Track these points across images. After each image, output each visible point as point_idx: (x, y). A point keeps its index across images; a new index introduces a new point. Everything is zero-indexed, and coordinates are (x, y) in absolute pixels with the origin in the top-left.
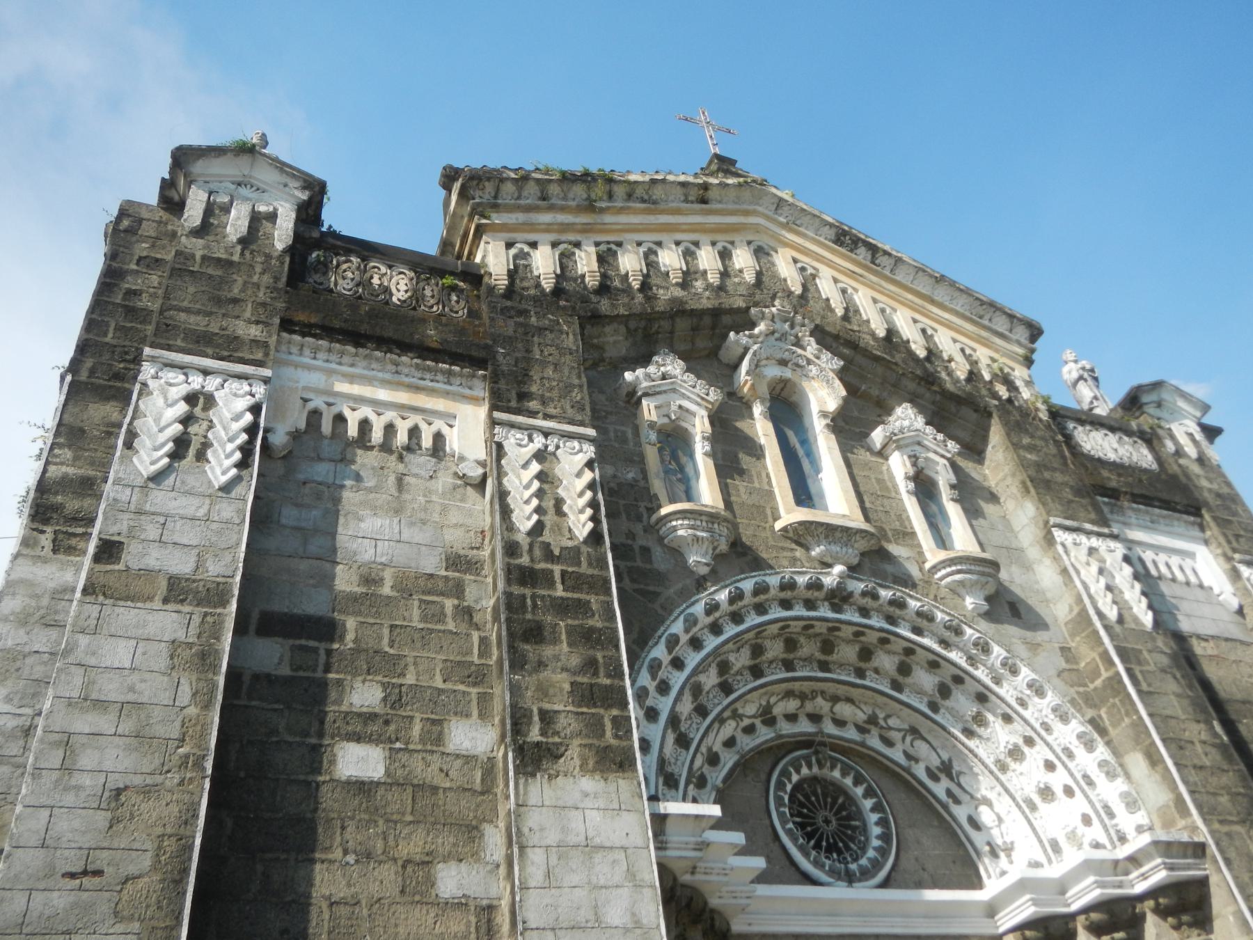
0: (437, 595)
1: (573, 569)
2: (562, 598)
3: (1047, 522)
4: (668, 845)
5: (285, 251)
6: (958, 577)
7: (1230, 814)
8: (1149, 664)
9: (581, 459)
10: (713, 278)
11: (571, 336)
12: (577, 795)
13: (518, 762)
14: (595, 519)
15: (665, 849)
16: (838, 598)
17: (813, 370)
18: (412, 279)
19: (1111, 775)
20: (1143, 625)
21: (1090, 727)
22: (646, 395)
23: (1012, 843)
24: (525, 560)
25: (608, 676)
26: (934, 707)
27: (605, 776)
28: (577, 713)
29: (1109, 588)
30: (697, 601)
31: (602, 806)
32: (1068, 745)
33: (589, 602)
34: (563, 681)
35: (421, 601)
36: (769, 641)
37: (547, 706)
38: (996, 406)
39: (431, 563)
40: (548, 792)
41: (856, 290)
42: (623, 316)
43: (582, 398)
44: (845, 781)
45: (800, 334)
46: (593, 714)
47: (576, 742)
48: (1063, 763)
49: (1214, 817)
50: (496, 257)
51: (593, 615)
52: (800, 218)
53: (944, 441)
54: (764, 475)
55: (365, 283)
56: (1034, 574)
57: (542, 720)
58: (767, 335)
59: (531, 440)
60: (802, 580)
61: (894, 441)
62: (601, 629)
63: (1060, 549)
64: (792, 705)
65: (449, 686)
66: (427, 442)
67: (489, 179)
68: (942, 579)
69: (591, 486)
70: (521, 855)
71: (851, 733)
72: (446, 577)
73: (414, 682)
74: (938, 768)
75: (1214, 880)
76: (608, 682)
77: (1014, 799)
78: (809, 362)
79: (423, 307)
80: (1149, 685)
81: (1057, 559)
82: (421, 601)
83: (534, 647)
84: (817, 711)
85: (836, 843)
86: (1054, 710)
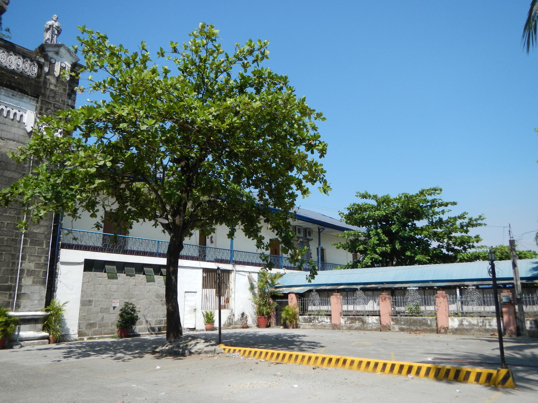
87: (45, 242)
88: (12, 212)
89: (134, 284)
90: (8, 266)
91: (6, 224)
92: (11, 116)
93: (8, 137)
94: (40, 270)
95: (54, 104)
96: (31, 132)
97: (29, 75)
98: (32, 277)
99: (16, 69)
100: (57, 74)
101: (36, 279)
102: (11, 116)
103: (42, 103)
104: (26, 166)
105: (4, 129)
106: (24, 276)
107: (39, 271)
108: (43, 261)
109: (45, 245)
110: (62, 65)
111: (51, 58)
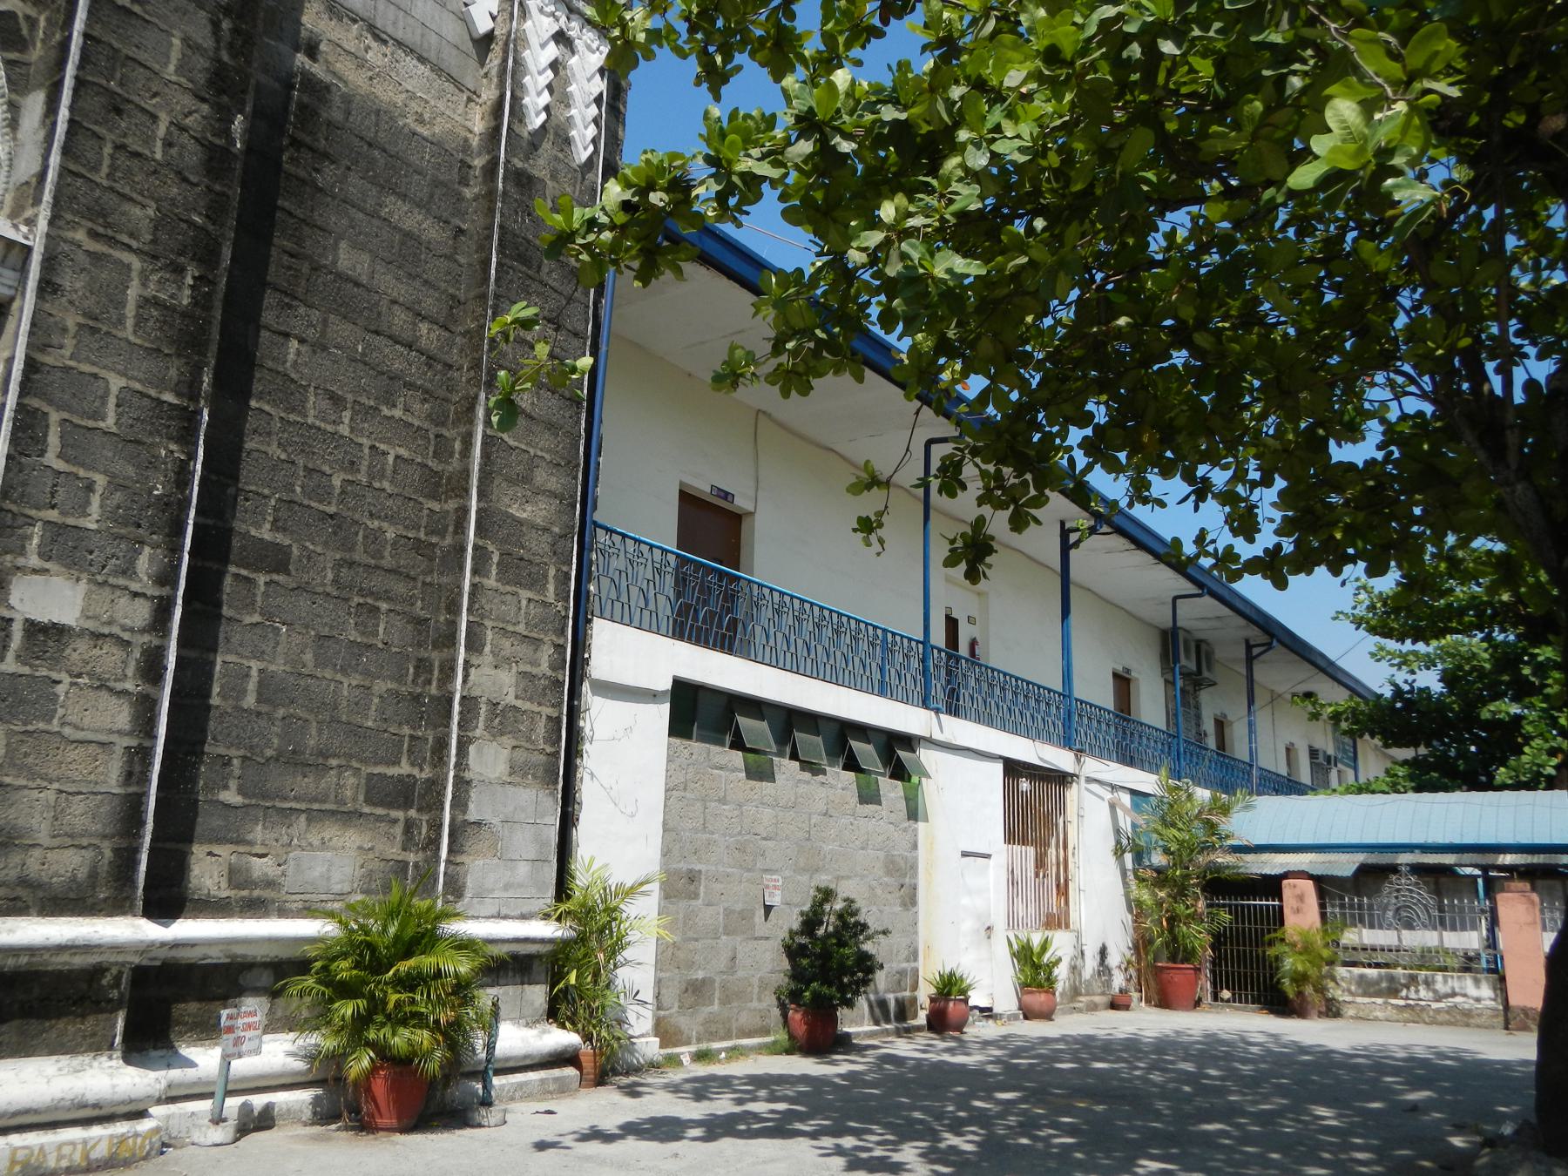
7: (131, 235)
49: (84, 222)
75: (15, 305)
87: (552, 572)
88: (417, 406)
89: (821, 807)
90: (400, 679)
91: (391, 459)
93: (399, 35)
94: (535, 708)
96: (489, 37)
98: (508, 741)
101: (521, 756)
104: (468, 193)
106: (478, 732)
107: (533, 715)
108: (544, 668)
109: (551, 588)
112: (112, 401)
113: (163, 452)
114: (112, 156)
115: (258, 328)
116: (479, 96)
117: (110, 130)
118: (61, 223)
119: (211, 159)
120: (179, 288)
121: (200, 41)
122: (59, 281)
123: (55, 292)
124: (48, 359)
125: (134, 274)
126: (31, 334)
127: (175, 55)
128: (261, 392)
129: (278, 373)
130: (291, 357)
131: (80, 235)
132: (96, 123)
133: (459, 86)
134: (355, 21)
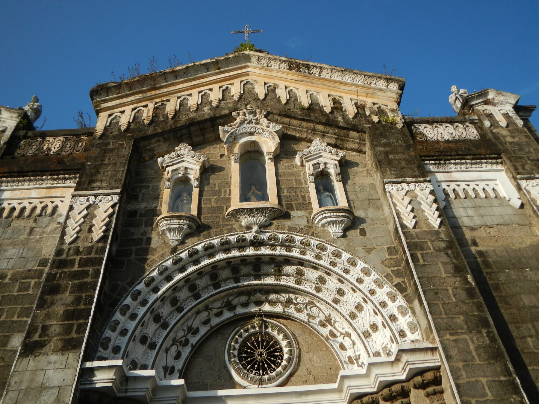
0: (29, 278)
1: (87, 256)
2: (75, 271)
3: (383, 181)
4: (93, 382)
5: (4, 144)
6: (324, 221)
7: (462, 329)
8: (430, 249)
9: (111, 203)
10: (215, 104)
11: (127, 148)
12: (45, 363)
13: (23, 351)
14: (106, 231)
15: (92, 384)
16: (257, 243)
17: (266, 134)
18: (62, 142)
19: (404, 314)
20: (434, 228)
21: (395, 288)
22: (167, 166)
23: (359, 355)
24: (64, 257)
25: (85, 304)
26: (318, 290)
27: (64, 352)
28: (61, 325)
29: (412, 211)
30: (170, 258)
31: (56, 367)
32: (385, 300)
33: (89, 270)
34: (59, 309)
35: (20, 282)
36: (221, 271)
37: (47, 323)
38: (369, 127)
39: (33, 266)
40: (32, 363)
41: (298, 89)
42: (159, 133)
43: (122, 176)
44: (273, 333)
45: (259, 118)
46: (69, 324)
47: (55, 338)
48: (380, 312)
50: (102, 122)
51: (88, 276)
52: (270, 63)
53: (337, 152)
54: (228, 190)
55: (39, 149)
56: (383, 210)
57: (42, 330)
58: (240, 123)
59: (88, 200)
60: (233, 239)
61: (305, 158)
62: (90, 282)
63: (388, 194)
64: (243, 299)
65: (20, 319)
66: (49, 210)
67: (101, 90)
68: (318, 223)
69: (110, 216)
70: (6, 395)
71: (279, 309)
72: (36, 270)
73: (3, 319)
74: (325, 320)
76: (83, 307)
77: (357, 332)
78: (263, 129)
79: (63, 153)
80: (424, 261)
81: (388, 200)
82: (20, 282)
83: (52, 296)
84: (259, 299)
85: (263, 365)
86: (375, 282)
92: (483, 195)
93: (496, 223)
95: (528, 158)
97: (470, 139)
99: (451, 139)
100: (503, 123)
102: (483, 195)
103: (511, 161)
105: (483, 213)
110: (502, 112)
111: (483, 111)
112: (486, 388)
113: (512, 400)
114: (443, 308)
115: (514, 340)
116: (532, 224)
117: (438, 301)
118: (441, 335)
119: (468, 293)
120: (484, 338)
121: (446, 261)
122: (450, 354)
123: (451, 358)
124: (461, 381)
125: (469, 341)
126: (452, 375)
127: (442, 269)
128: (530, 362)
129: (530, 352)
130: (531, 344)
131: (448, 336)
132: (434, 301)
133: (524, 225)
134: (481, 227)
